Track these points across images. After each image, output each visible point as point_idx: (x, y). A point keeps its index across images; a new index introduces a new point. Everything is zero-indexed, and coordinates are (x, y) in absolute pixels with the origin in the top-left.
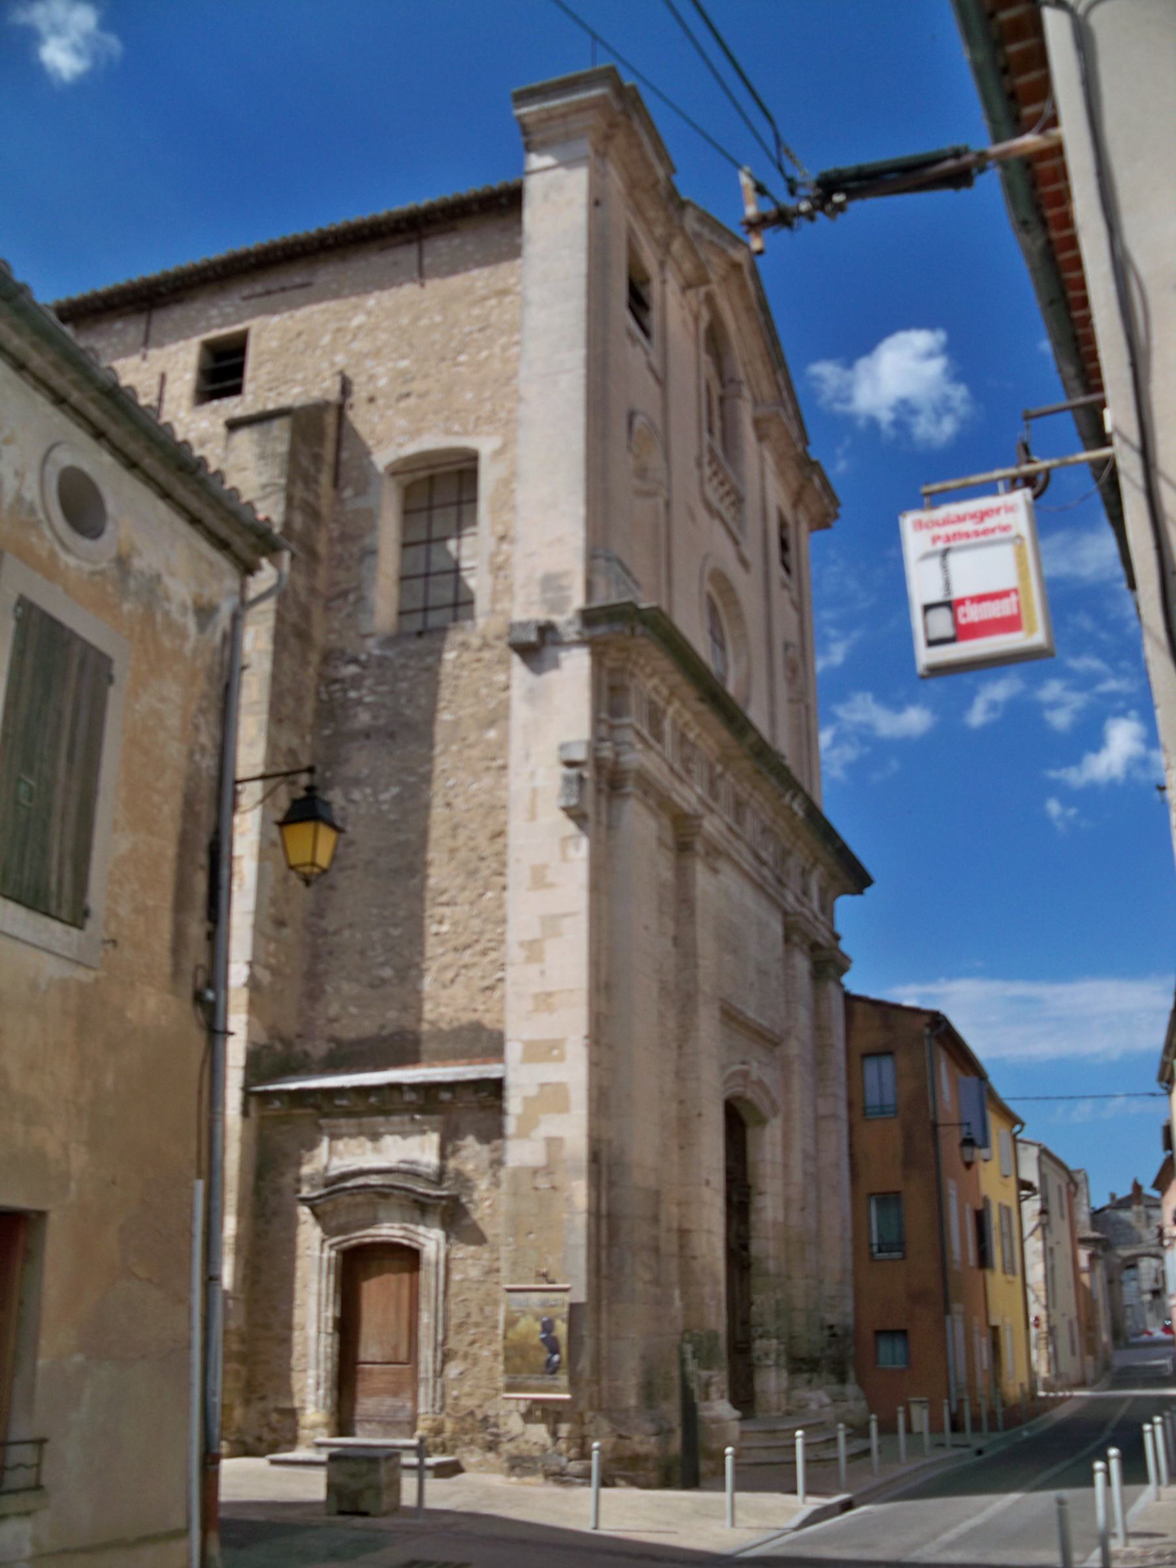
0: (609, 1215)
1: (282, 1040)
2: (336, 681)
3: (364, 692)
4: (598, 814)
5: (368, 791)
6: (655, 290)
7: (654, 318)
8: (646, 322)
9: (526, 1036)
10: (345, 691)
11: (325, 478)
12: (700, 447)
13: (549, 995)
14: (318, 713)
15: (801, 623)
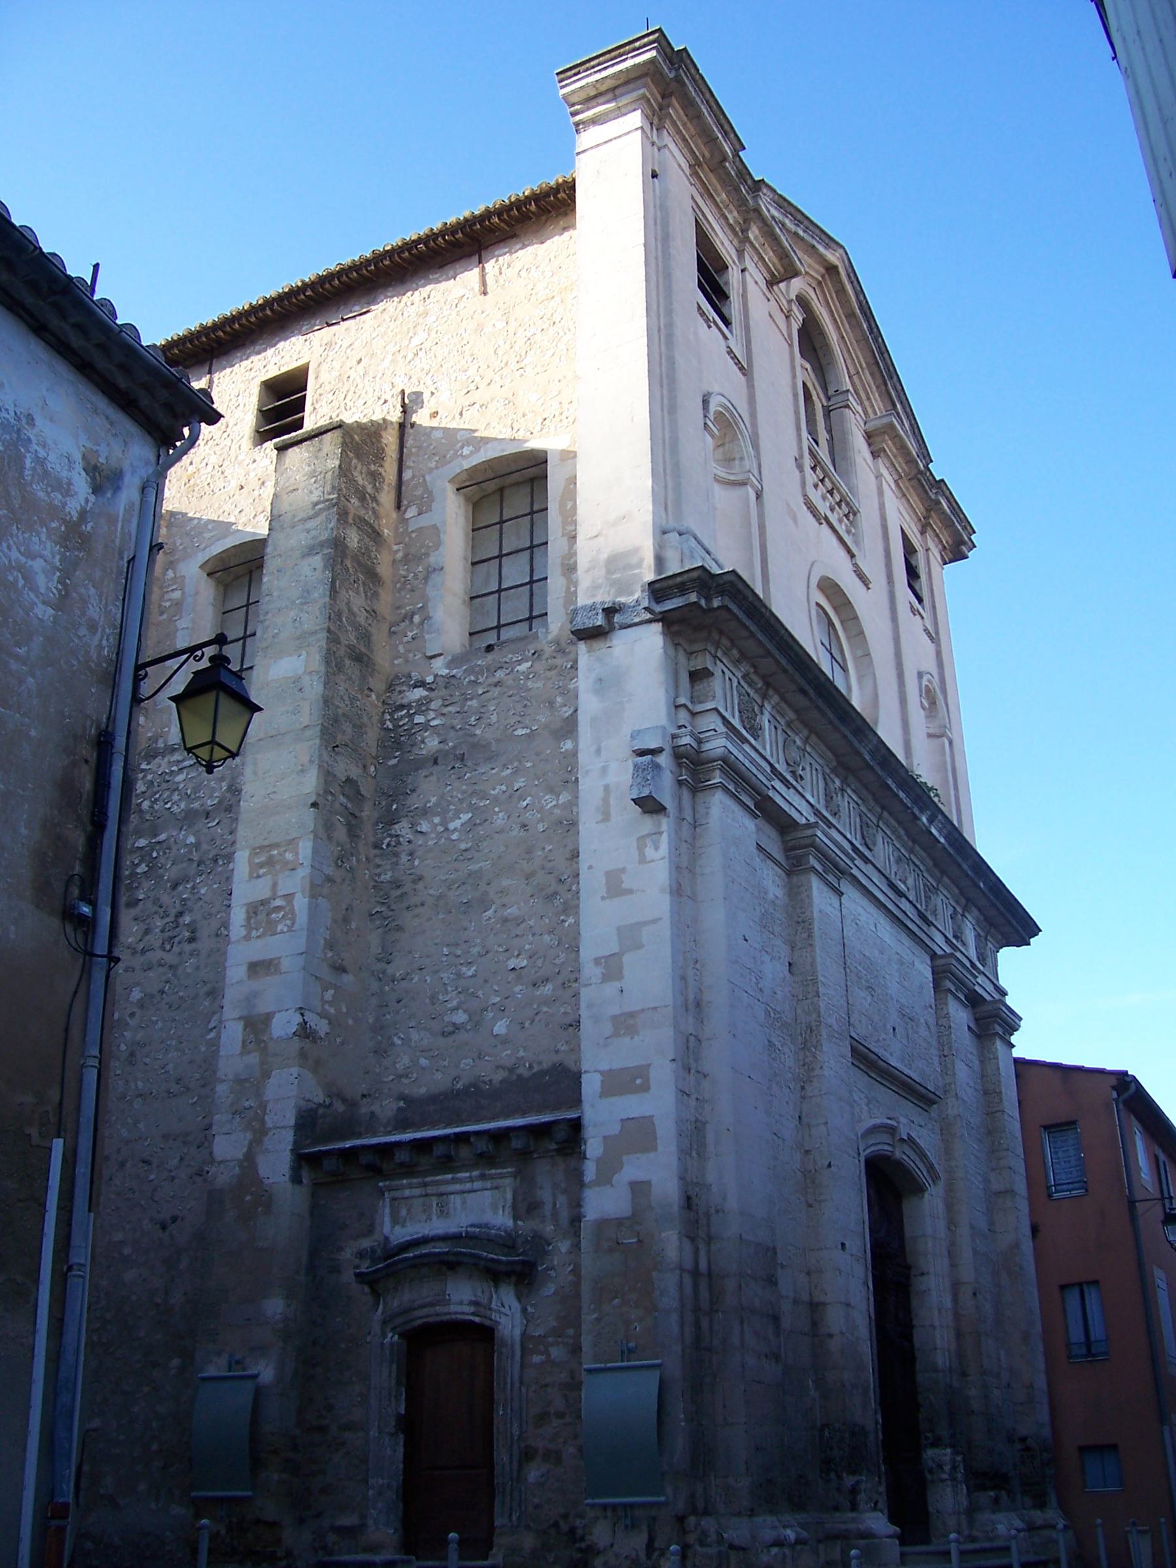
0: (710, 1275)
1: (344, 1100)
2: (402, 707)
3: (432, 715)
4: (680, 809)
5: (437, 820)
6: (733, 277)
7: (734, 309)
8: (725, 311)
9: (605, 1066)
10: (411, 716)
11: (387, 498)
12: (800, 449)
13: (632, 1015)
14: (381, 744)
15: (939, 654)
